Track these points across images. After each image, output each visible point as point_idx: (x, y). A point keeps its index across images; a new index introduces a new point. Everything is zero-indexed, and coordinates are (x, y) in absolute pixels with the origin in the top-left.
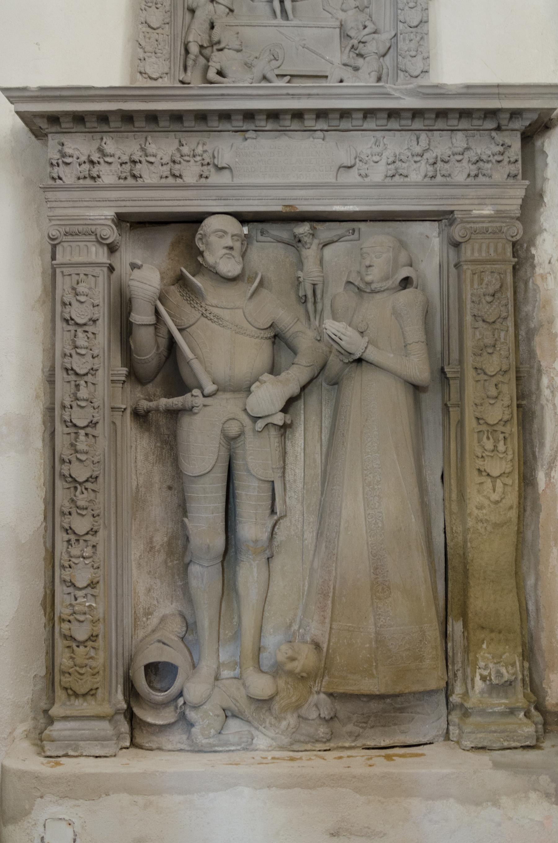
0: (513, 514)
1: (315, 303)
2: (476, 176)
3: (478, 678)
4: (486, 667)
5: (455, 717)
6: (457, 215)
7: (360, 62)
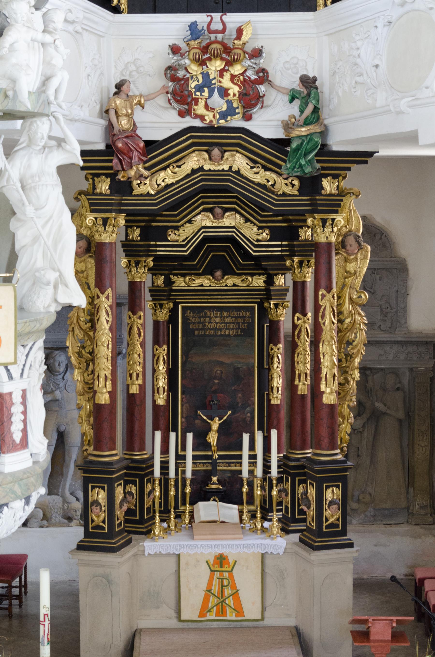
0: (428, 457)
1: (371, 393)
2: (420, 358)
3: (417, 504)
4: (419, 501)
5: (410, 516)
6: (414, 369)
7: (386, 318)
